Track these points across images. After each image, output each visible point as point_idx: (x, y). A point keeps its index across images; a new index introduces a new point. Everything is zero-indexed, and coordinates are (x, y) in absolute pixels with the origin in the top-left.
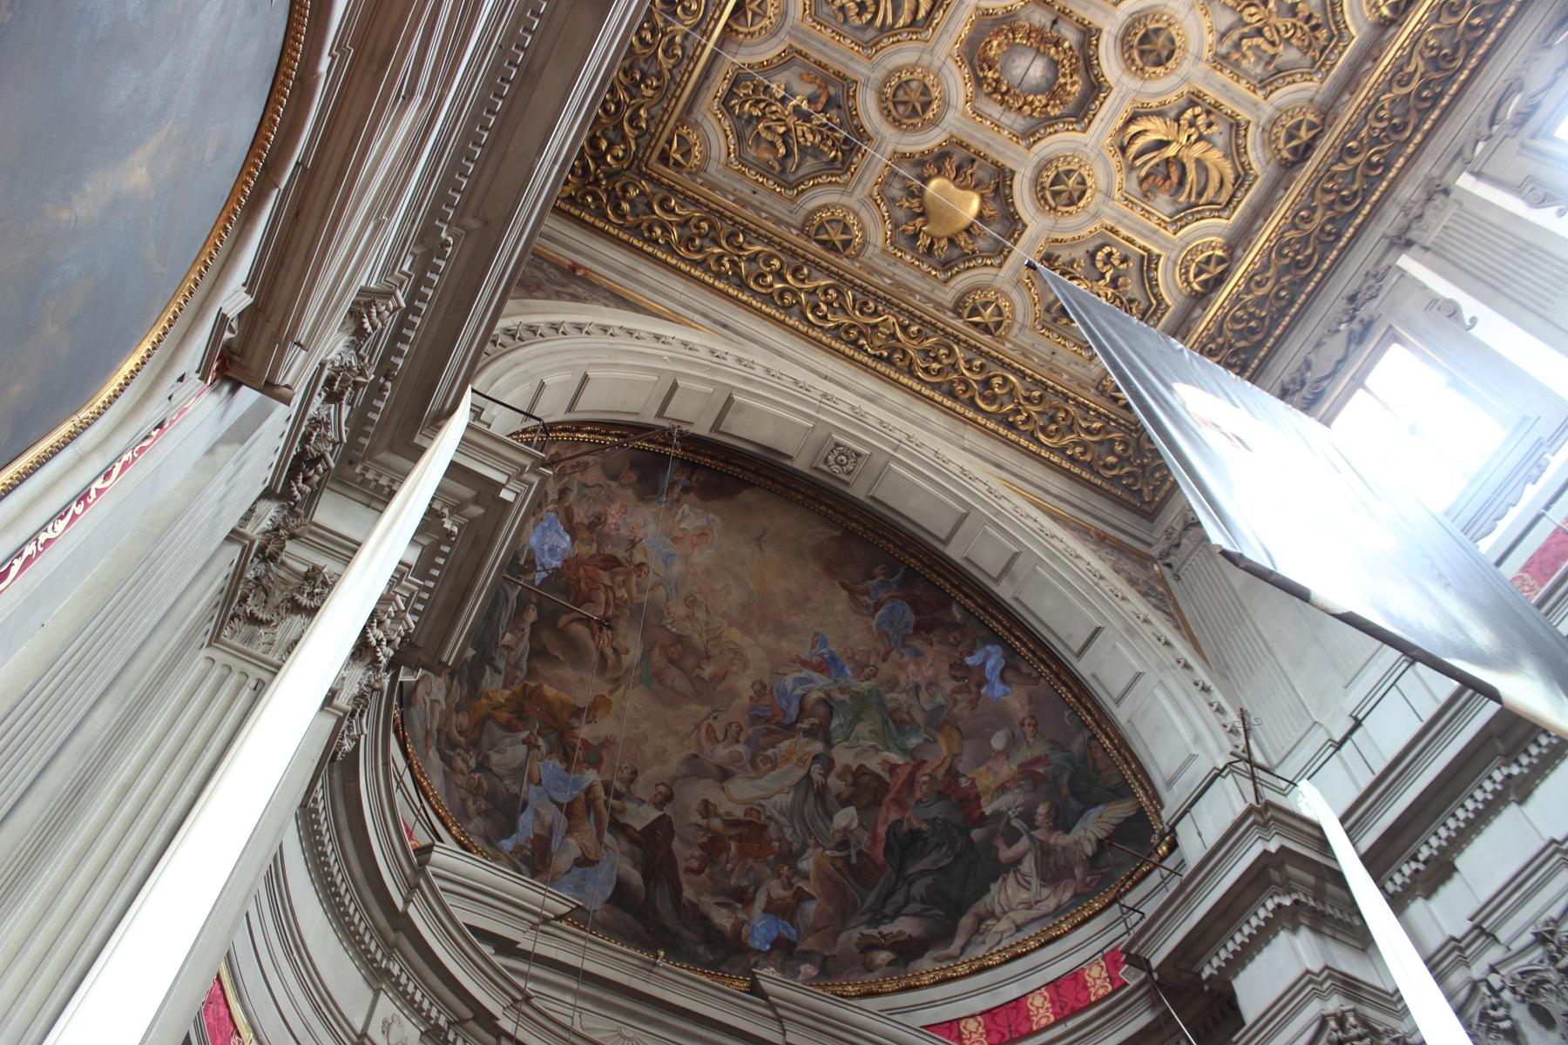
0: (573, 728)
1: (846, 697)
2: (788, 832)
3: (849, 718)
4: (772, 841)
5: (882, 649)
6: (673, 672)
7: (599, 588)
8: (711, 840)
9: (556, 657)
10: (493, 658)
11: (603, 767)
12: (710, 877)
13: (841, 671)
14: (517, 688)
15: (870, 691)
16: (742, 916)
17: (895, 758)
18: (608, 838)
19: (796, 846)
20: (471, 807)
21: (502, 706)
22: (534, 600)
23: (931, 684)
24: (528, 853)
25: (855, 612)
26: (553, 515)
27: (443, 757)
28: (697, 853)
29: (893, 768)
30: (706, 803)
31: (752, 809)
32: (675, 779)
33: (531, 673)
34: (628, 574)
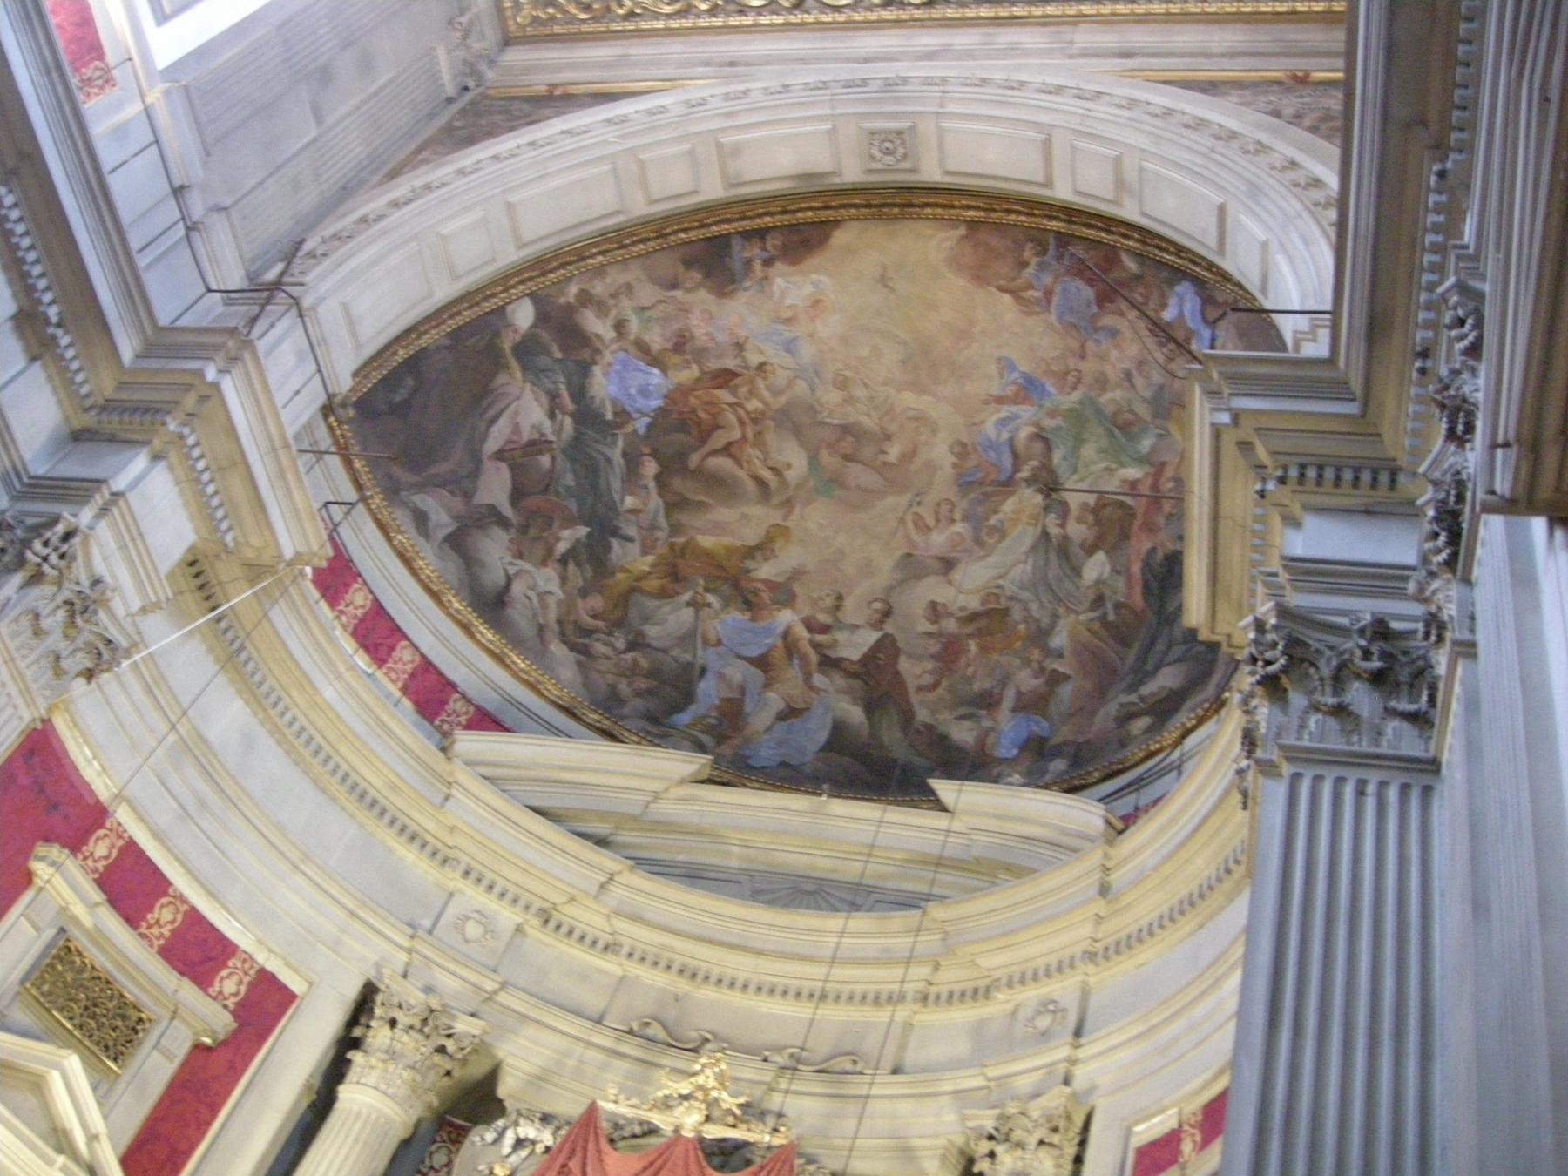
0: (749, 571)
1: (1059, 421)
2: (1034, 607)
3: (1070, 444)
4: (1017, 623)
5: (1075, 344)
6: (854, 469)
7: (723, 410)
8: (946, 646)
9: (700, 502)
10: (617, 528)
11: (799, 601)
12: (950, 689)
13: (1043, 392)
14: (662, 549)
15: (1081, 403)
16: (987, 723)
17: (1133, 472)
18: (819, 680)
19: (1045, 621)
20: (623, 687)
21: (650, 573)
22: (646, 450)
23: (1141, 363)
24: (713, 721)
25: (1029, 314)
26: (622, 355)
27: (573, 647)
28: (930, 665)
29: (1133, 485)
30: (933, 606)
31: (988, 595)
32: (890, 589)
33: (675, 529)
34: (751, 382)
